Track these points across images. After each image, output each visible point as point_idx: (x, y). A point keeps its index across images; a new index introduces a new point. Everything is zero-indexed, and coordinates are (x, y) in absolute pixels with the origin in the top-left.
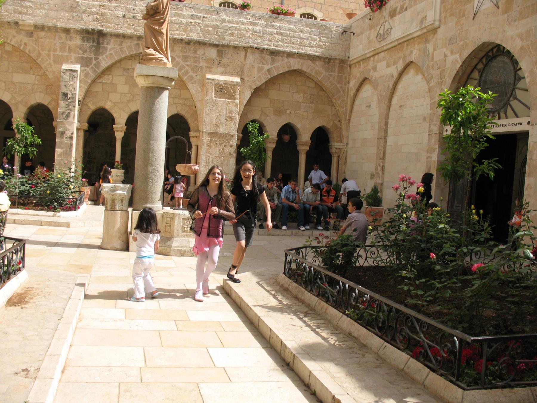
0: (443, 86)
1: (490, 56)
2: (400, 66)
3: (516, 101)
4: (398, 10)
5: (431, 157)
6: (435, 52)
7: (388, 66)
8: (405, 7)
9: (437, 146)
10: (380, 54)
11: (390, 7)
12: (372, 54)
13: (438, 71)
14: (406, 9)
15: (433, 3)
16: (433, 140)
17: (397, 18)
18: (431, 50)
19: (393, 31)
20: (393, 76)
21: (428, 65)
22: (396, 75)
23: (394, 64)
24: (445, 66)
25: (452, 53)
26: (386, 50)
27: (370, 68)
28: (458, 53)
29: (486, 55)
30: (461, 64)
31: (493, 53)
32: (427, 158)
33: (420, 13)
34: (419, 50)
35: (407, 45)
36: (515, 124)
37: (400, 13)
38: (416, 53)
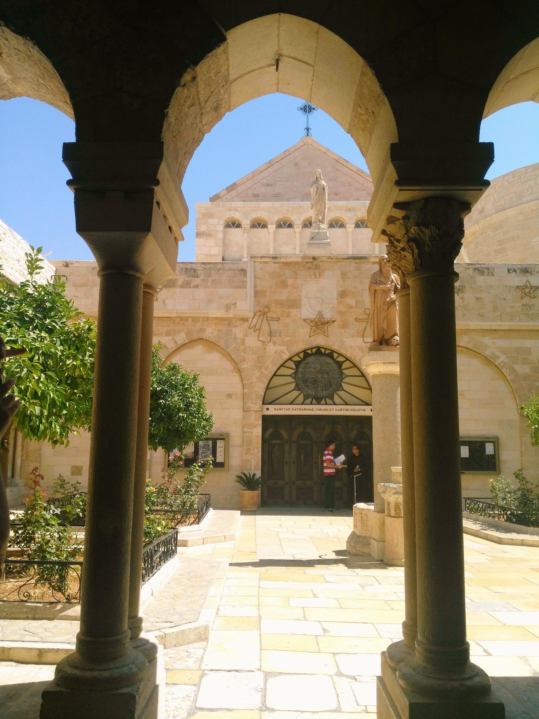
0: (263, 370)
2: (181, 338)
3: (343, 392)
4: (180, 282)
5: (252, 433)
6: (246, 338)
9: (261, 422)
13: (255, 356)
14: (197, 286)
15: (246, 294)
16: (253, 417)
17: (178, 290)
21: (236, 346)
23: (168, 334)
24: (265, 353)
28: (284, 345)
29: (305, 351)
30: (289, 356)
31: (312, 352)
32: (243, 433)
34: (218, 330)
35: (193, 321)
36: (357, 410)
37: (182, 287)
38: (212, 332)
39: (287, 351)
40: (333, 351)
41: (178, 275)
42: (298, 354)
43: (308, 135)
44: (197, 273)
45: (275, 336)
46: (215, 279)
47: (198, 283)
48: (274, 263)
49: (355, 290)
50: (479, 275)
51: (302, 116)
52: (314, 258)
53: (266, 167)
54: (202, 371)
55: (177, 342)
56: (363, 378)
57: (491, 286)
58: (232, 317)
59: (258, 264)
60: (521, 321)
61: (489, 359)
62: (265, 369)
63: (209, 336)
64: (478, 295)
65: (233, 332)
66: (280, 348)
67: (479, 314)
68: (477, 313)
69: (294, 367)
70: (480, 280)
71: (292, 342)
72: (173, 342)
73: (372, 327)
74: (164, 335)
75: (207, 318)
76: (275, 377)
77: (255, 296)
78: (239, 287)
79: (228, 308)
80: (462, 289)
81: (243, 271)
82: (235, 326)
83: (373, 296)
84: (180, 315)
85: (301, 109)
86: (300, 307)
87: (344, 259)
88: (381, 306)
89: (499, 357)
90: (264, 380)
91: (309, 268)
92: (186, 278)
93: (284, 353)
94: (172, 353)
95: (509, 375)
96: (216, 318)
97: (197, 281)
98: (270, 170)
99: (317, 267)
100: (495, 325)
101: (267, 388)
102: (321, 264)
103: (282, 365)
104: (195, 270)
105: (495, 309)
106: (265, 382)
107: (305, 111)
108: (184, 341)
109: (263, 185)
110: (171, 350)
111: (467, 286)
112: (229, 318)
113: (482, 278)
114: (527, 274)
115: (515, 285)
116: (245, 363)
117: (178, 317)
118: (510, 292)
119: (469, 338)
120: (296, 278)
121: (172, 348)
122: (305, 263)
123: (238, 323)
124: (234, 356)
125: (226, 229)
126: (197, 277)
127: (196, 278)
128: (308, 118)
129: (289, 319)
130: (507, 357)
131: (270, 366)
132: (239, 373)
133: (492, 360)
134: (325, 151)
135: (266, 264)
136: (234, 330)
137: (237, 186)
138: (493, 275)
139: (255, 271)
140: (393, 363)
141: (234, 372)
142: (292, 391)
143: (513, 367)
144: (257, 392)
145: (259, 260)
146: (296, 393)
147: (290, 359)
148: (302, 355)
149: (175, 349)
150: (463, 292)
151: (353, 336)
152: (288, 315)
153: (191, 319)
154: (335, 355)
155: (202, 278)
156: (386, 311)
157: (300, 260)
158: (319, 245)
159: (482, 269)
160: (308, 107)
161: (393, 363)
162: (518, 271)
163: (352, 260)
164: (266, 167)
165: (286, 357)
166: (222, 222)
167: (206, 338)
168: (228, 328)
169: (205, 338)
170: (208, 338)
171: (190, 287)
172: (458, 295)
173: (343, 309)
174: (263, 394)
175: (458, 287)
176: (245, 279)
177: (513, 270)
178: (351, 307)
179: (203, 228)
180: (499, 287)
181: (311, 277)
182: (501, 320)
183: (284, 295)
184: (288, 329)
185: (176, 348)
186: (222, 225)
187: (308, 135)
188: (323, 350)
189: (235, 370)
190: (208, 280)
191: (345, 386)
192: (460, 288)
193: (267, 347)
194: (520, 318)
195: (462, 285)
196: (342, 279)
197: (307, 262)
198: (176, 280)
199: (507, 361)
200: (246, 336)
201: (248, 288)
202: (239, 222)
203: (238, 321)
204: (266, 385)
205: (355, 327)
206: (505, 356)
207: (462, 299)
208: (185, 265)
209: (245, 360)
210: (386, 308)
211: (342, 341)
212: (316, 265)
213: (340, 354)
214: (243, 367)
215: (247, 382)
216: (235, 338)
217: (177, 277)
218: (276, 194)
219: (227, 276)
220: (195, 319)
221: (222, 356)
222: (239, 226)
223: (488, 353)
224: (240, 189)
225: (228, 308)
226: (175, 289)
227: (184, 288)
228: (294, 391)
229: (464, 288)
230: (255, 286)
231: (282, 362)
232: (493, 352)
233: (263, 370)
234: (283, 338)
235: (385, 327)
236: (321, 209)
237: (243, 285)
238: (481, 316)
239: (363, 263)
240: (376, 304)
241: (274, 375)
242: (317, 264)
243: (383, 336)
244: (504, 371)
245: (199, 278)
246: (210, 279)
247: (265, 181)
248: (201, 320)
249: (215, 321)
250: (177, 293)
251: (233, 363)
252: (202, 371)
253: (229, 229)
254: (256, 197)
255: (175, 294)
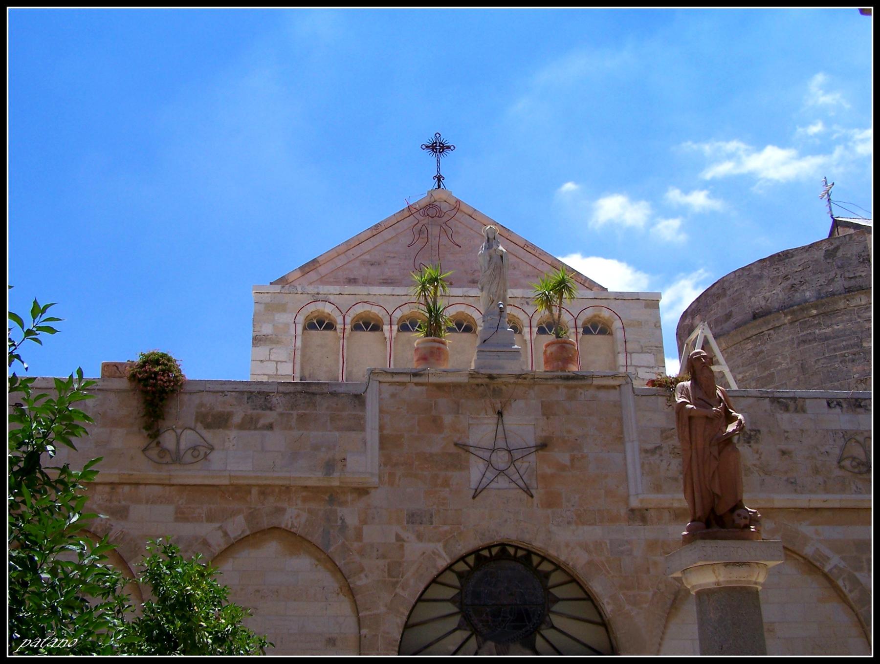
0: (399, 590)
1: (485, 557)
2: (237, 526)
4: (237, 419)
6: (365, 528)
7: (181, 516)
8: (262, 422)
10: (141, 487)
11: (202, 405)
12: (115, 479)
14: (270, 427)
17: (233, 434)
18: (352, 520)
19: (214, 456)
20: (205, 543)
21: (343, 543)
22: (218, 542)
23: (210, 519)
25: (420, 537)
26: (173, 485)
27: (95, 507)
28: (439, 541)
29: (476, 552)
30: (449, 561)
33: (323, 449)
34: (310, 511)
37: (241, 427)
38: (298, 516)
39: (445, 552)
40: (529, 553)
41: (234, 405)
42: (463, 558)
43: (439, 186)
44: (270, 402)
45: (421, 523)
46: (304, 413)
47: (272, 421)
48: (417, 384)
49: (568, 437)
50: (782, 412)
51: (430, 158)
52: (491, 377)
53: (369, 234)
54: (277, 592)
55: (229, 533)
56: (589, 603)
57: (802, 431)
58: (337, 486)
59: (385, 387)
60: (860, 493)
61: (811, 563)
62: (403, 589)
63: (292, 521)
64: (784, 447)
65: (340, 514)
66: (431, 546)
67: (787, 480)
68: (785, 478)
69: (457, 583)
70: (784, 419)
71: (455, 534)
72: (220, 533)
73: (689, 491)
74: (204, 518)
75: (288, 488)
76: (420, 604)
77: (382, 446)
78: (350, 429)
79: (329, 467)
80: (755, 435)
81: (359, 399)
82: (342, 504)
83: (687, 429)
84: (236, 482)
85: (427, 147)
86: (468, 468)
87: (546, 379)
88: (704, 448)
89: (828, 558)
90: (402, 609)
91: (483, 396)
92: (250, 412)
93: (440, 556)
94: (218, 555)
95: (851, 591)
96: (306, 487)
97: (270, 417)
98: (377, 240)
99: (497, 392)
100: (817, 500)
101: (407, 626)
102: (504, 387)
103: (434, 581)
104: (266, 394)
105: (816, 471)
106: (403, 614)
107: (434, 151)
108: (243, 532)
109: (364, 264)
110: (217, 550)
111: (763, 429)
112: (331, 487)
113: (786, 416)
114: (858, 410)
115: (843, 428)
116: (362, 575)
117: (232, 485)
118: (835, 441)
119: (775, 524)
120: (458, 413)
121: (219, 545)
122: (473, 386)
123: (350, 498)
124: (340, 563)
125: (305, 331)
126: (271, 409)
127: (268, 412)
128: (438, 161)
129: (448, 489)
130: (842, 558)
131: (412, 582)
132: (351, 597)
133: (818, 564)
134: (470, 213)
135: (401, 387)
136: (341, 511)
137: (318, 265)
138: (804, 411)
139: (381, 399)
140: (744, 564)
141: (341, 594)
142: (455, 630)
143: (855, 577)
144: (388, 633)
145: (389, 379)
146: (465, 634)
147: (449, 568)
148: (471, 560)
149: (223, 547)
150: (757, 441)
151: (569, 523)
152: (446, 483)
153: (257, 488)
154: (535, 560)
155: (280, 410)
156: (716, 459)
157: (464, 379)
158: (499, 354)
159: (784, 401)
160: (438, 144)
161: (744, 564)
162: (845, 405)
163: (561, 382)
164: (370, 235)
165: (443, 563)
166: (301, 319)
167: (287, 526)
168: (330, 507)
169: (283, 526)
170: (290, 526)
171: (256, 429)
172: (750, 446)
173: (549, 471)
174: (399, 637)
175: (748, 432)
176: (361, 413)
177: (835, 403)
178: (562, 468)
179: (267, 329)
180: (817, 432)
181: (486, 411)
182: (826, 491)
183: (437, 444)
184: (445, 510)
185: (226, 546)
186: (300, 325)
187: (439, 186)
188: (511, 551)
189: (343, 591)
190: (292, 414)
191: (556, 620)
192: (752, 433)
193: (406, 545)
194: (857, 487)
195: (754, 428)
196: (544, 415)
197: (478, 385)
198: (230, 415)
199: (842, 564)
200: (366, 523)
201: (368, 429)
202: (329, 320)
203: (349, 494)
204: (405, 618)
205: (573, 506)
206: (840, 556)
207: (757, 452)
208: (248, 387)
209: (362, 570)
210: (716, 453)
211: (549, 532)
212: (494, 390)
213: (544, 558)
214: (359, 583)
215: (368, 613)
216: (344, 527)
217: (231, 410)
218: (387, 279)
219: (327, 408)
220: (265, 491)
221: (317, 563)
222: (330, 326)
223: (808, 551)
224: (323, 270)
225: (329, 467)
226: (227, 432)
227: (245, 429)
228: (458, 632)
229: (758, 434)
230: (381, 428)
231: (435, 573)
232: (817, 549)
233: (399, 590)
234: (436, 527)
235: (717, 490)
236: (498, 292)
237: (359, 425)
238: (792, 483)
239: (580, 388)
240: (694, 444)
241: (420, 599)
242: (497, 389)
243: (713, 510)
244: (840, 583)
245: (274, 410)
246: (294, 413)
247: (367, 257)
248: (277, 490)
249: (304, 494)
250: (231, 438)
251: (339, 576)
252: (277, 592)
253: (313, 332)
254: (352, 281)
255: (228, 440)
